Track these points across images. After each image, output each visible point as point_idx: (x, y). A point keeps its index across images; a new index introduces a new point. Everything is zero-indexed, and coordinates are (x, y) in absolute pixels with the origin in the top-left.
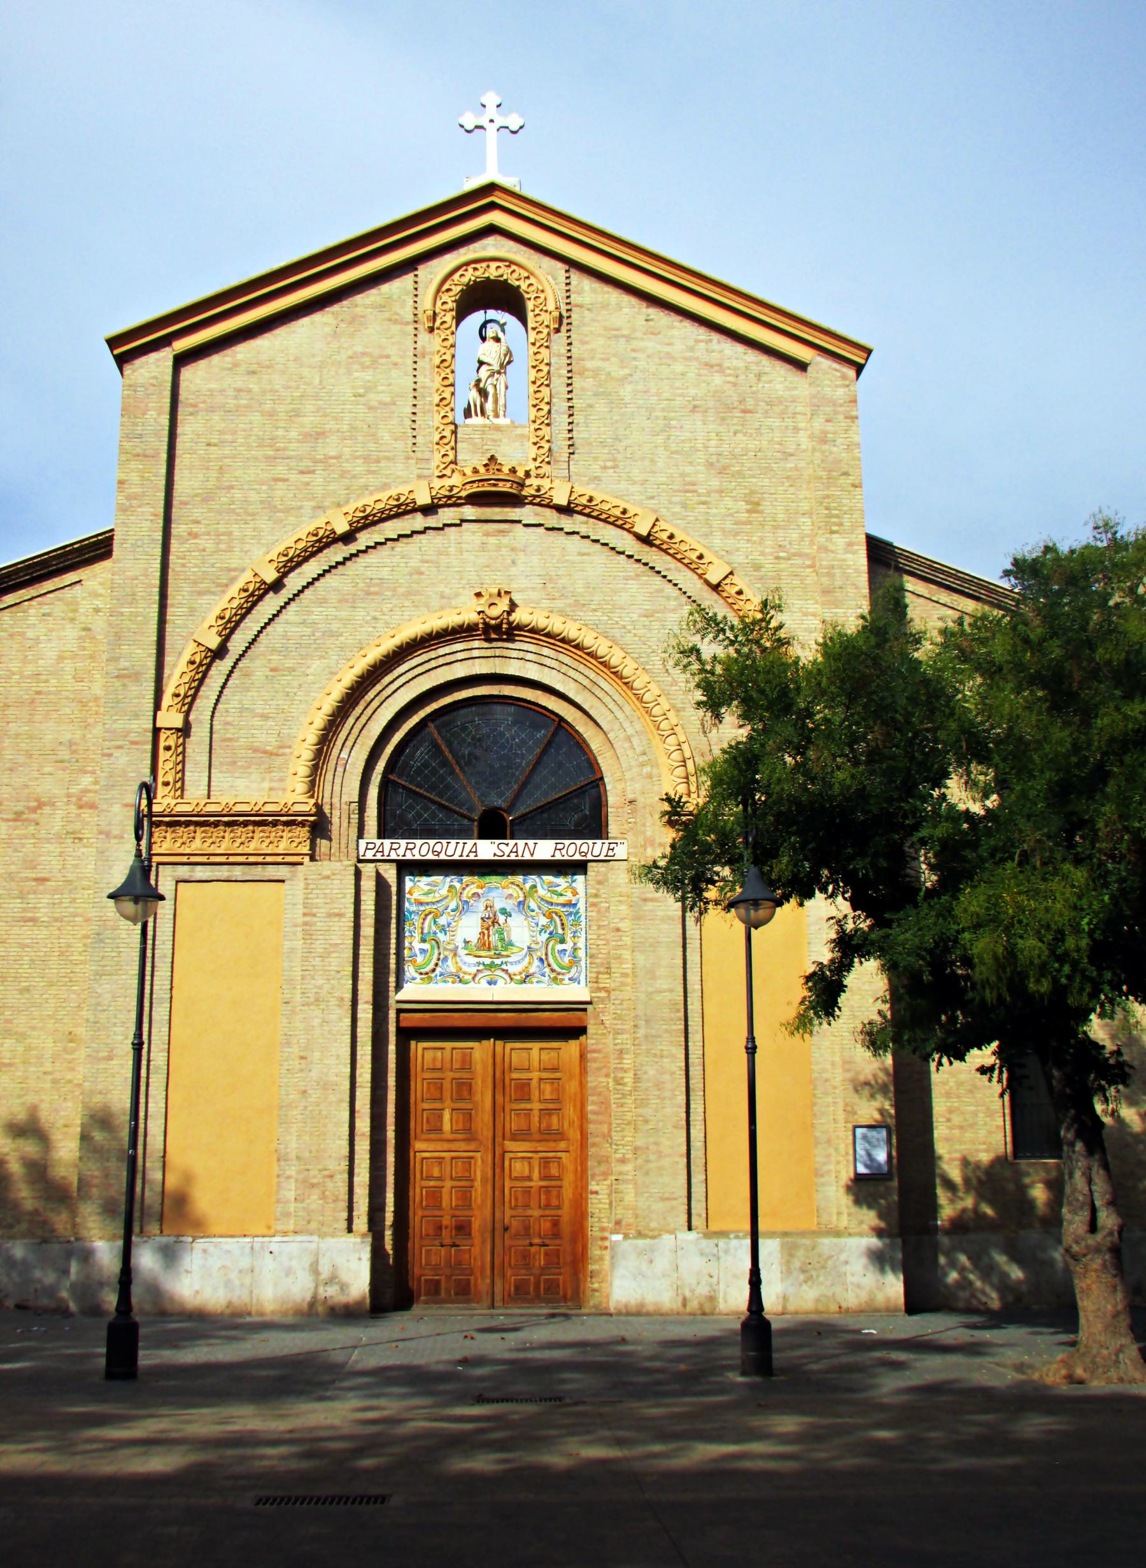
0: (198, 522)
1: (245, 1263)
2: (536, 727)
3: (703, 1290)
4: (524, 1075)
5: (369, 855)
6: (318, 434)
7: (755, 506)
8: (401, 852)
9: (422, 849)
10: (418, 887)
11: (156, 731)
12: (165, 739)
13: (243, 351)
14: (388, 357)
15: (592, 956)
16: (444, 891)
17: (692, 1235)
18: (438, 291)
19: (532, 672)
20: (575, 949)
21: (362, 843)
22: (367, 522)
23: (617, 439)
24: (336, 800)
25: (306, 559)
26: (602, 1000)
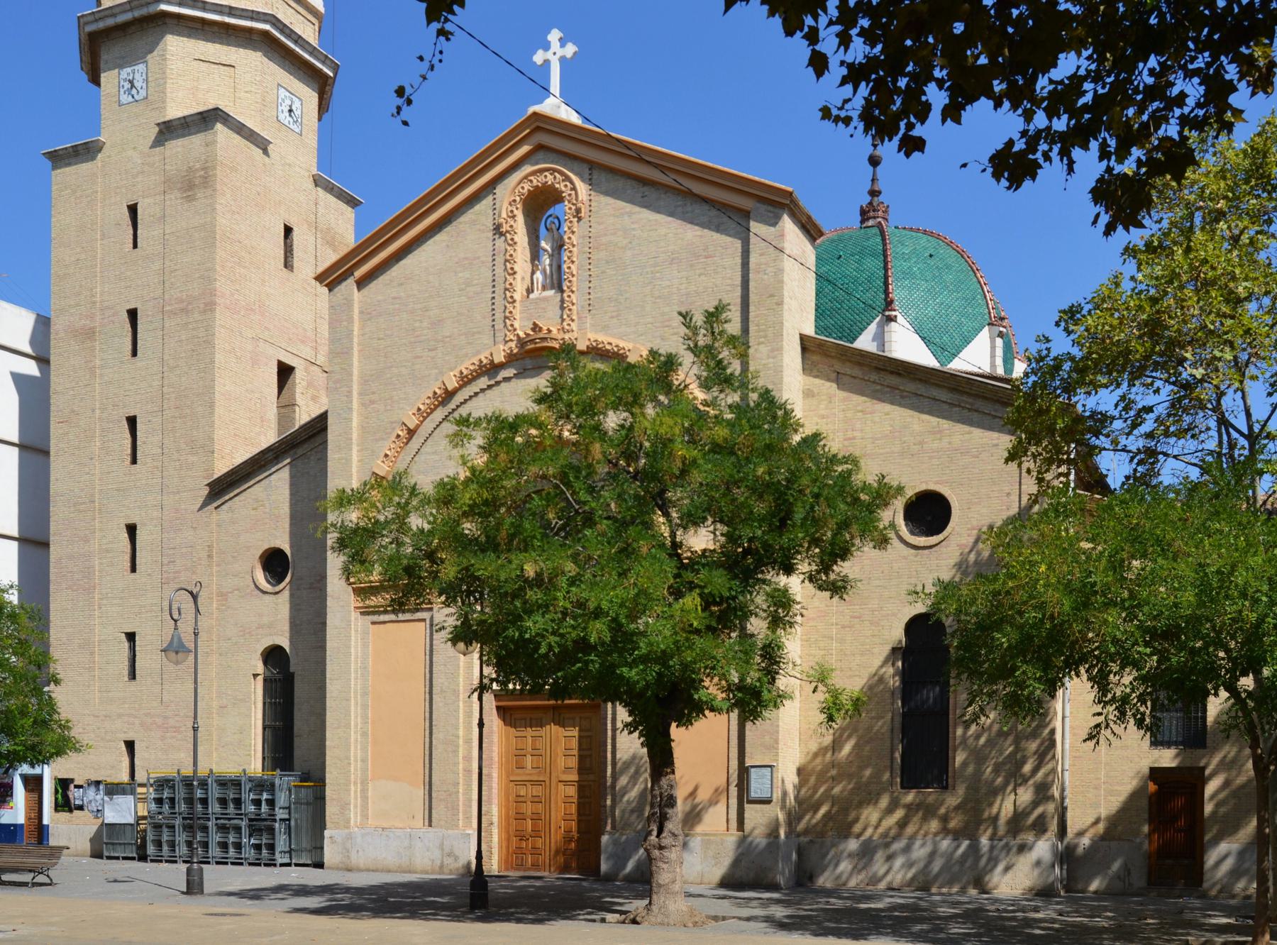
6: (439, 321)
13: (396, 271)
14: (479, 258)
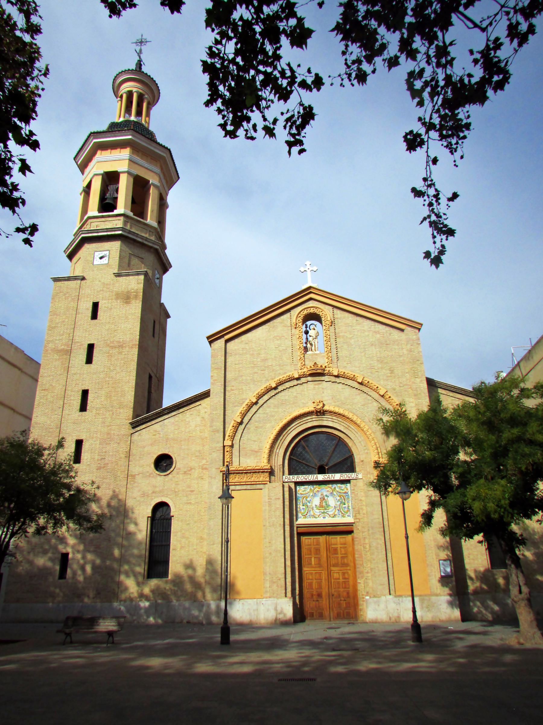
0: (233, 386)
1: (255, 607)
2: (333, 440)
3: (396, 615)
4: (336, 546)
5: (286, 480)
7: (392, 372)
8: (295, 479)
9: (301, 478)
10: (301, 490)
11: (224, 446)
12: (227, 449)
13: (243, 337)
15: (354, 508)
16: (308, 490)
17: (391, 597)
18: (297, 317)
19: (331, 424)
20: (348, 506)
21: (284, 477)
22: (281, 383)
23: (350, 355)
24: (276, 465)
25: (264, 395)
26: (358, 522)
